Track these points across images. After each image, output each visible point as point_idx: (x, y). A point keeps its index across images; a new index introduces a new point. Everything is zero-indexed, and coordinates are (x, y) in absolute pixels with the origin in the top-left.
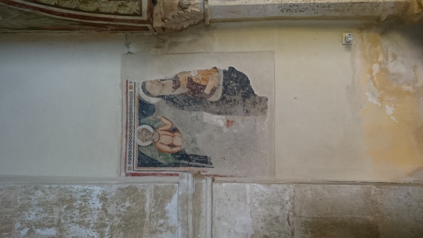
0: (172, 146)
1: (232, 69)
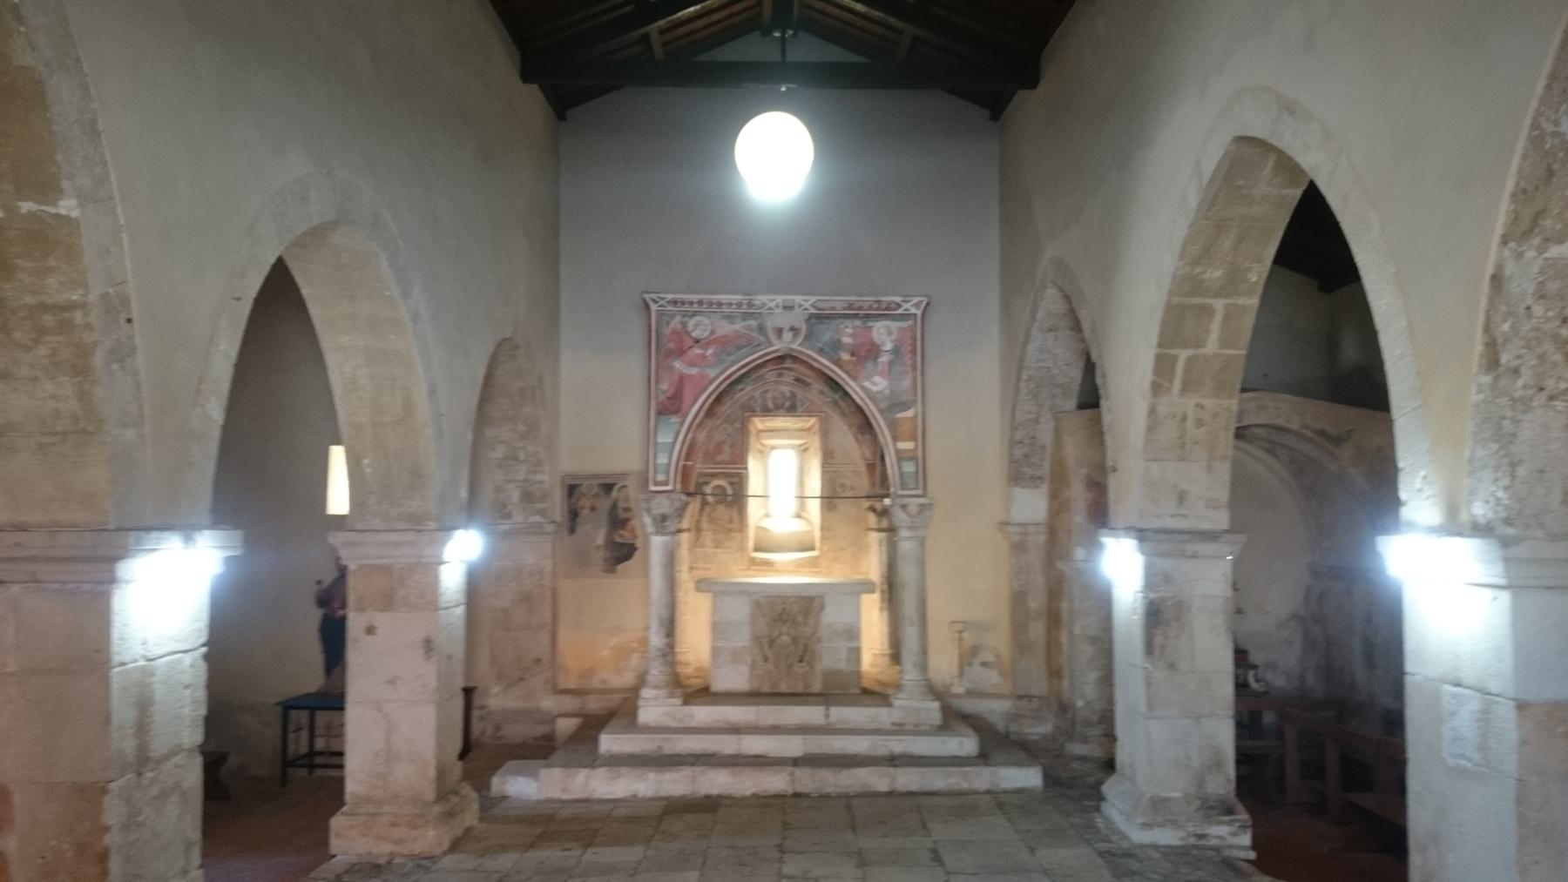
0: (582, 508)
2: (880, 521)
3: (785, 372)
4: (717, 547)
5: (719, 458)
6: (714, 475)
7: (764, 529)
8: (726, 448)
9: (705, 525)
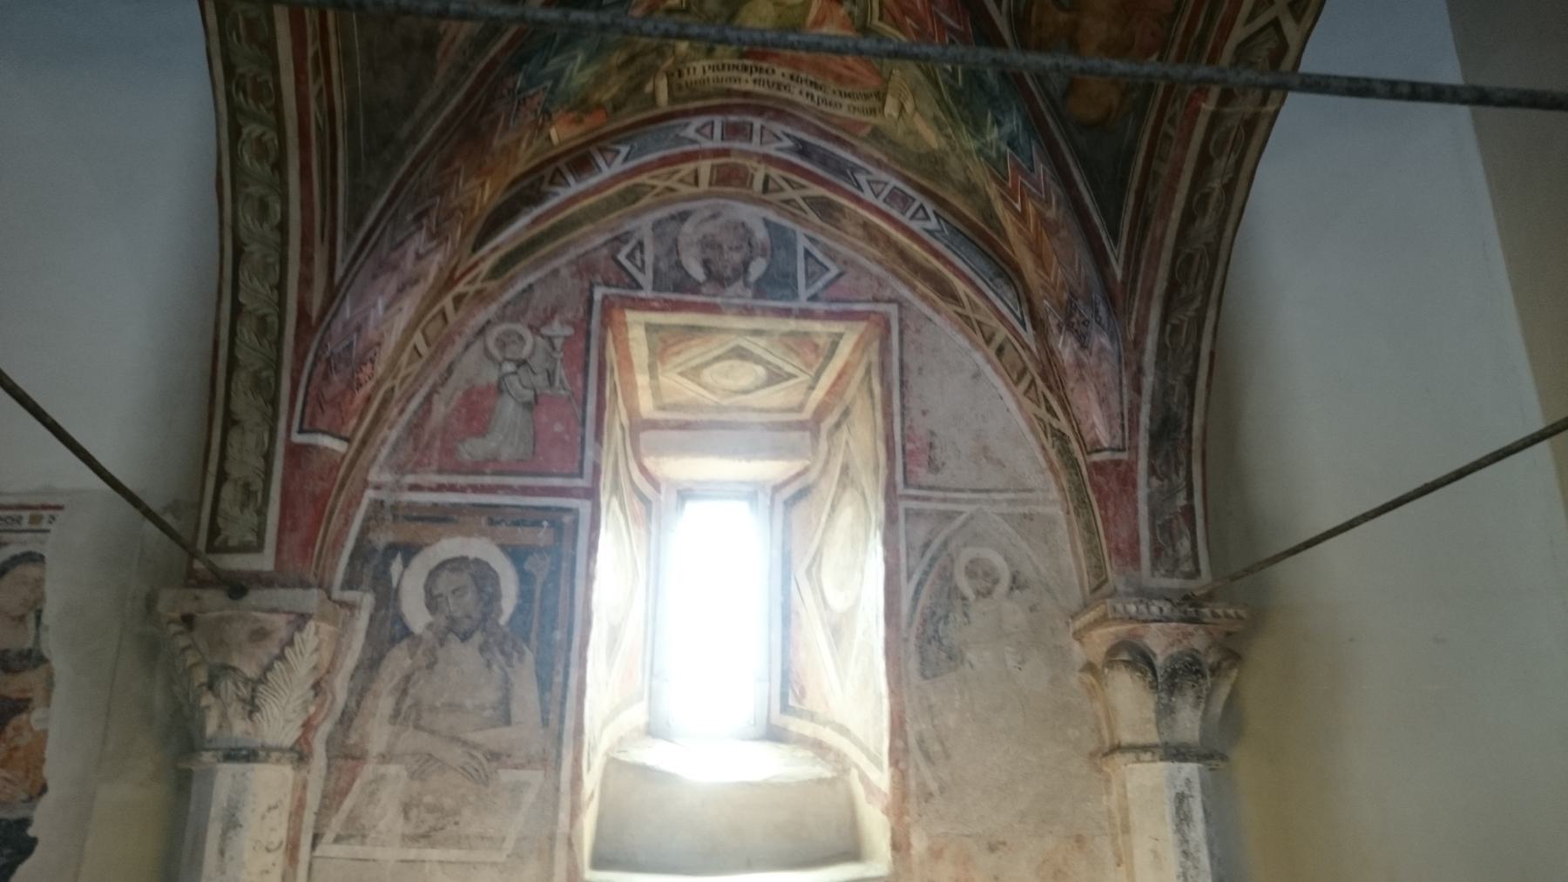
1: (27, 847)
2: (1165, 712)
3: (757, 123)
4: (425, 837)
5: (472, 449)
6: (442, 517)
7: (644, 771)
8: (508, 409)
9: (377, 733)
